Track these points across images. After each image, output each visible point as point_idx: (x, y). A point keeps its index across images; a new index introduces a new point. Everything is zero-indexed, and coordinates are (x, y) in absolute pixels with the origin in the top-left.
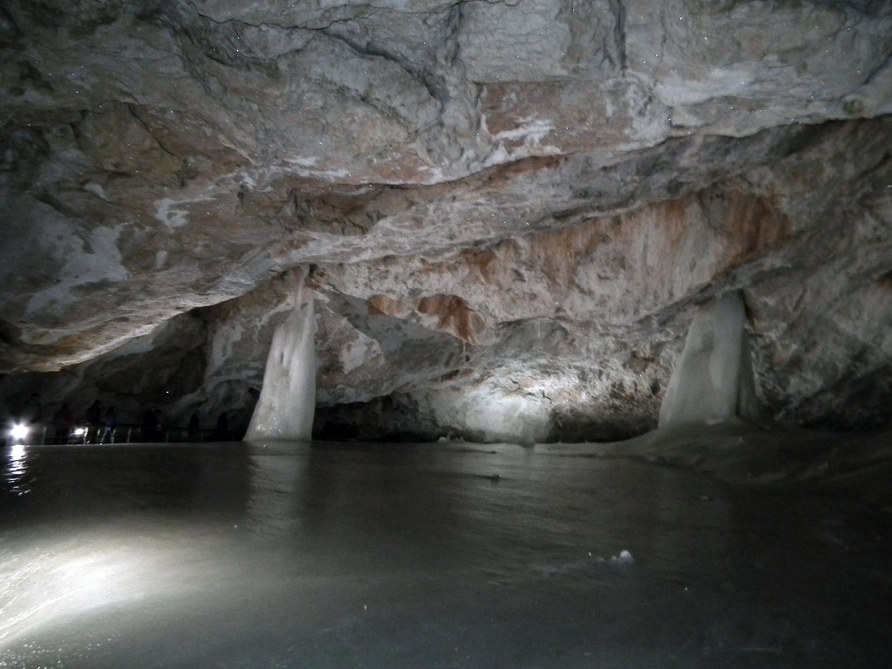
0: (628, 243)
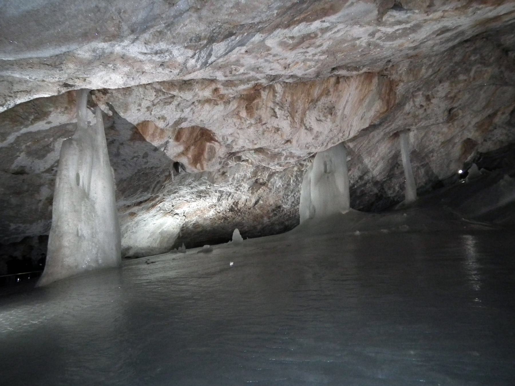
0: (339, 97)
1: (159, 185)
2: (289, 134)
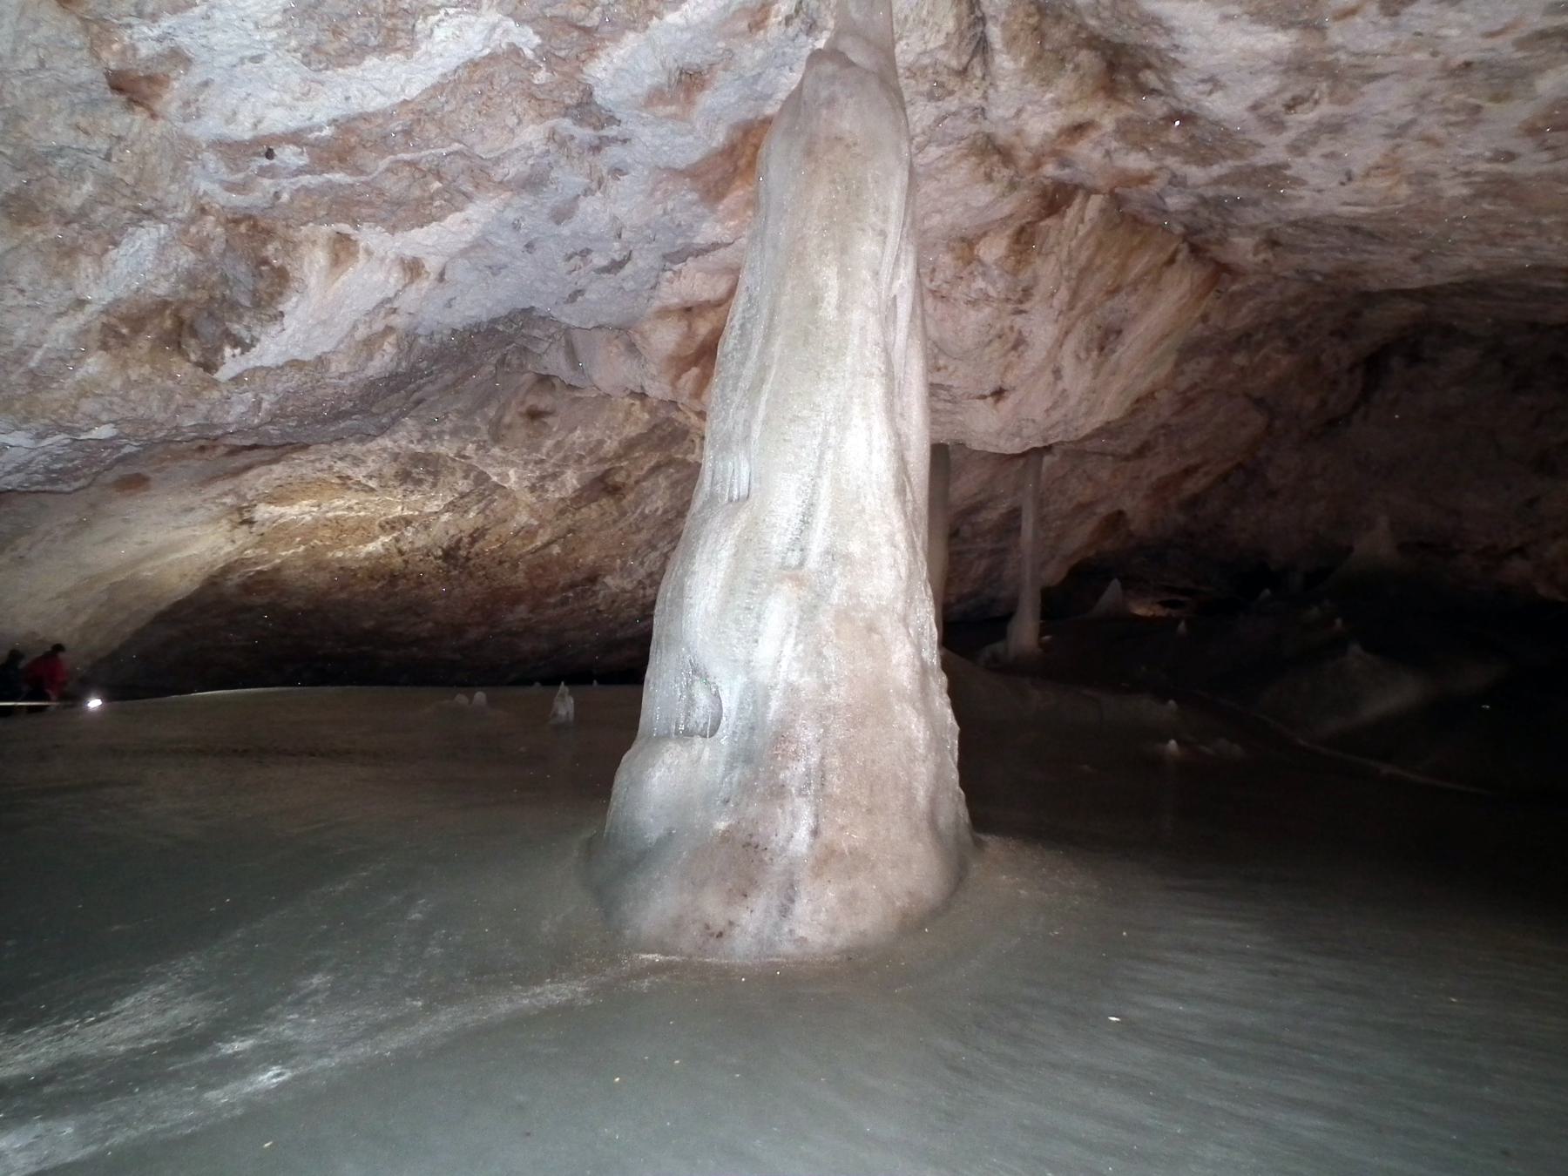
0: (1147, 305)
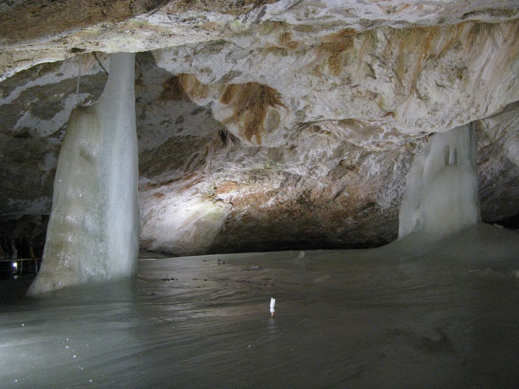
1: (196, 160)
2: (391, 103)
